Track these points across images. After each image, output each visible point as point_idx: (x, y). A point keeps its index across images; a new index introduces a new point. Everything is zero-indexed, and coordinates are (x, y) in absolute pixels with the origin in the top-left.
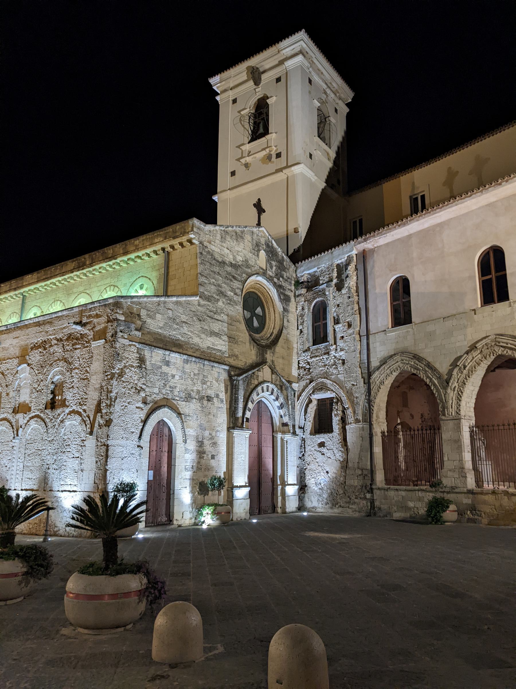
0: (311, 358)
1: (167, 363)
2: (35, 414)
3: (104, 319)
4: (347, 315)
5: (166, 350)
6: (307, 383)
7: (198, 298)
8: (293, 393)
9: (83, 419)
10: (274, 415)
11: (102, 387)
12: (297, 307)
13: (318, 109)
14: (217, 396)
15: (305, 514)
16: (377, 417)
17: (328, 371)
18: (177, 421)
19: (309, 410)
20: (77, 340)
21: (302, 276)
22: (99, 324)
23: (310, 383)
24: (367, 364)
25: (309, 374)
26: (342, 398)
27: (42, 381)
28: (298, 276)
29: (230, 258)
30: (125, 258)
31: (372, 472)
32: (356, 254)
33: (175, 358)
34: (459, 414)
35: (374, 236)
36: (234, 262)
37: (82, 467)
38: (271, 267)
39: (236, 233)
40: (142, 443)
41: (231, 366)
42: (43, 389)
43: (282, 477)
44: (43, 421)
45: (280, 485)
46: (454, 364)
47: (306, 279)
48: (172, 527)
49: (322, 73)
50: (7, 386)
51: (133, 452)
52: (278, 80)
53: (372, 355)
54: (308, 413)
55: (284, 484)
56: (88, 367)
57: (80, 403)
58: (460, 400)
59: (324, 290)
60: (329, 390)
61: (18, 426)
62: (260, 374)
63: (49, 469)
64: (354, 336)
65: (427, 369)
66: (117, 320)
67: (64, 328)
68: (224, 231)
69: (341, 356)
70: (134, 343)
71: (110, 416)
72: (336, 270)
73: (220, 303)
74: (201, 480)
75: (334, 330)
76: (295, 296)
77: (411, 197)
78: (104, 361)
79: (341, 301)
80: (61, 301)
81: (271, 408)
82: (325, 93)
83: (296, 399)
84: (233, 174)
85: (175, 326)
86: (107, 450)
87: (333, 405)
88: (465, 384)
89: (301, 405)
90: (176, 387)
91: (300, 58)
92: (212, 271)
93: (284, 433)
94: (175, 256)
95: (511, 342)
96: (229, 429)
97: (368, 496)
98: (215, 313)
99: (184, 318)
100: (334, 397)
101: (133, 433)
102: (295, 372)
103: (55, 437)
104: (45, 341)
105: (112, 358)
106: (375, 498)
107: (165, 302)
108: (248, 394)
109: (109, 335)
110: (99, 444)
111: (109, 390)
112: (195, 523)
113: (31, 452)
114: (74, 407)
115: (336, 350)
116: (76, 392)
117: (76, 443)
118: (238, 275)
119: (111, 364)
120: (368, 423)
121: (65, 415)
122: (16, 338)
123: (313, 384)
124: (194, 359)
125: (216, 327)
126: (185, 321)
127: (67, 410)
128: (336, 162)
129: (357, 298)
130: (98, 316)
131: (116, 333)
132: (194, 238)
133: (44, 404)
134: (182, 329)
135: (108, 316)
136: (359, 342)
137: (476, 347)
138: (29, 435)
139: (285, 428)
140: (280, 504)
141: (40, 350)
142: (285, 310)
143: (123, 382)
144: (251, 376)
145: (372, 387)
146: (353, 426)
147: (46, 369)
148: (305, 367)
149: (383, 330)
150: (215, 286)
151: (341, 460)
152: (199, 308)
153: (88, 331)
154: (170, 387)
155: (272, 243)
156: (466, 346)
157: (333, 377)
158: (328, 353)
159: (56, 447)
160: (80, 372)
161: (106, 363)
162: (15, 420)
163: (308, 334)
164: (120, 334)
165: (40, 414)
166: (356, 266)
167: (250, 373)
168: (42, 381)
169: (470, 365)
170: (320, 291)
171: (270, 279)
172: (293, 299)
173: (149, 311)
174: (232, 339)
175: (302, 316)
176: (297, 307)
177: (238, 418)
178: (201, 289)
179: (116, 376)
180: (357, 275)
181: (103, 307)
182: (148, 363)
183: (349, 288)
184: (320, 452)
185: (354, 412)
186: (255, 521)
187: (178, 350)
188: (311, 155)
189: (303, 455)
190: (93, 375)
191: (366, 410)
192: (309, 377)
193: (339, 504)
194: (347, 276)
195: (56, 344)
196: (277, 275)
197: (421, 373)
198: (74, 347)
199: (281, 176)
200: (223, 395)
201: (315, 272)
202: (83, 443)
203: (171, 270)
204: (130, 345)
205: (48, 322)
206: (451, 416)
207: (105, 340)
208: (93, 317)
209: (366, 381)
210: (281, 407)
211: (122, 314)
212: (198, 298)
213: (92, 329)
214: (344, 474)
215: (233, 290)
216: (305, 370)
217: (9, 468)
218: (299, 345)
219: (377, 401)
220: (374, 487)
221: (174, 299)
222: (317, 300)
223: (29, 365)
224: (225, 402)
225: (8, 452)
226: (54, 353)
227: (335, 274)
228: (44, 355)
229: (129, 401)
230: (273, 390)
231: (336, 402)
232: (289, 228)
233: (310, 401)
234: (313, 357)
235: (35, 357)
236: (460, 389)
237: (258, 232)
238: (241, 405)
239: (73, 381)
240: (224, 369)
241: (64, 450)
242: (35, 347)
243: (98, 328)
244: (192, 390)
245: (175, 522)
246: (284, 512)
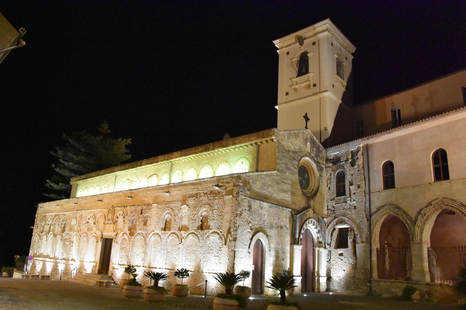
0: (335, 204)
1: (262, 208)
2: (192, 232)
3: (232, 184)
4: (358, 180)
5: (261, 201)
6: (332, 218)
7: (276, 172)
8: (325, 224)
9: (220, 236)
10: (314, 236)
11: (231, 220)
12: (327, 174)
13: (336, 59)
14: (285, 226)
15: (331, 293)
16: (375, 240)
17: (345, 212)
18: (266, 239)
19: (334, 234)
20: (216, 194)
21: (330, 156)
22: (228, 187)
23: (334, 219)
24: (369, 209)
26: (354, 228)
27: (195, 214)
28: (328, 155)
29: (292, 148)
30: (234, 147)
31: (371, 271)
32: (363, 146)
33: (265, 205)
34: (422, 241)
35: (373, 137)
36: (294, 150)
37: (220, 261)
38: (313, 152)
39: (295, 133)
40: (250, 251)
41: (292, 209)
42: (196, 219)
43: (318, 272)
44: (197, 235)
45: (317, 276)
46: (419, 213)
47: (332, 158)
48: (264, 295)
49: (338, 39)
50: (174, 216)
51: (246, 255)
52: (314, 43)
53: (372, 205)
54: (333, 236)
55: (319, 276)
56: (223, 209)
58: (422, 233)
59: (343, 165)
60: (346, 224)
62: (308, 213)
63: (200, 261)
64: (361, 193)
65: (404, 215)
66: (239, 185)
67: (208, 187)
68: (289, 133)
69: (353, 204)
70: (247, 198)
72: (350, 154)
73: (287, 174)
74: (277, 272)
75: (350, 189)
76: (326, 167)
77: (392, 111)
78: (232, 207)
79: (354, 172)
80: (194, 168)
81: (312, 233)
82: (340, 49)
83: (326, 228)
84: (287, 94)
85: (266, 188)
86: (235, 254)
87: (348, 232)
88: (425, 224)
89: (329, 231)
90: (265, 221)
91: (326, 33)
92: (283, 156)
93: (319, 247)
94: (262, 147)
95: (451, 202)
96: (291, 244)
97: (368, 284)
98: (285, 180)
99: (270, 183)
100: (349, 228)
101: (246, 245)
102: (325, 212)
103: (204, 244)
104: (197, 194)
105: (237, 205)
106: (372, 286)
107: (261, 175)
108: (301, 225)
109: (234, 194)
110: (230, 250)
111: (236, 222)
112: (274, 294)
114: (215, 230)
115: (351, 200)
116: (216, 222)
117: (216, 249)
118: (296, 157)
119: (236, 208)
120: (369, 244)
122: (180, 190)
123: (336, 220)
124: (274, 206)
125: (285, 187)
126: (270, 184)
127: (211, 231)
128: (347, 88)
129: (363, 171)
130: (228, 183)
131: (239, 192)
132: (275, 139)
134: (268, 189)
135: (234, 183)
136: (365, 197)
137: (431, 204)
138: (188, 242)
139: (320, 244)
140: (316, 287)
142: (321, 176)
143: (242, 218)
144: (303, 215)
145: (371, 223)
146: (360, 245)
147: (198, 209)
148: (331, 209)
149: (378, 191)
150: (285, 164)
151: (353, 264)
152: (277, 177)
153: (222, 190)
154: (263, 221)
155: (313, 137)
156: (425, 203)
157: (349, 216)
158: (346, 202)
161: (233, 208)
162: (180, 234)
163: (333, 190)
164: (240, 193)
165: (194, 232)
166: (362, 153)
167: (303, 213)
168: (195, 214)
169: (428, 213)
170: (341, 165)
171: (312, 158)
172: (324, 169)
173: (254, 180)
174: (293, 193)
175: (330, 179)
176: (327, 174)
177: (296, 238)
178: (278, 167)
179: (239, 215)
180: (363, 158)
181: (231, 178)
182: (253, 208)
183: (359, 165)
184: (340, 259)
185: (361, 237)
186: (305, 295)
187: (266, 201)
188: (333, 86)
189: (330, 260)
190: (225, 214)
191: (368, 236)
192: (334, 215)
193: (351, 289)
194: (357, 159)
195: (203, 196)
196: (316, 156)
197: (400, 216)
198: (214, 198)
199: (316, 97)
200: (288, 226)
201: (338, 154)
203: (260, 155)
204: (245, 199)
205: (199, 184)
206: (417, 242)
207: (233, 196)
208: (225, 183)
209: (369, 219)
210: (318, 232)
211: (242, 182)
212: (276, 172)
213: (225, 189)
214: (354, 272)
215: (293, 166)
216: (331, 211)
217: (177, 259)
218: (328, 196)
219: (375, 231)
220: (372, 279)
221: (265, 173)
222: (339, 170)
223: (187, 205)
224: (289, 230)
225: (176, 250)
226: (202, 200)
227: (350, 157)
228: (196, 201)
229: (244, 228)
230: (314, 222)
231: (350, 231)
232: (322, 127)
233: (334, 229)
234: (337, 204)
235: (191, 201)
236: (422, 227)
237: (306, 132)
238: (298, 231)
239: (214, 216)
240: (289, 211)
241: (209, 252)
242: (191, 196)
243: (228, 189)
244: (273, 223)
245: (265, 293)
246: (319, 291)
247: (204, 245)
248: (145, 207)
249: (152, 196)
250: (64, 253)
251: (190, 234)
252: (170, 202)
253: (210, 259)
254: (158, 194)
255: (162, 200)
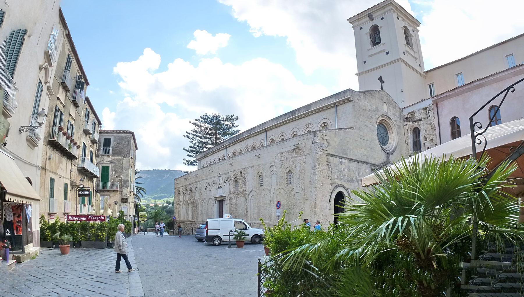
36: (371, 109)
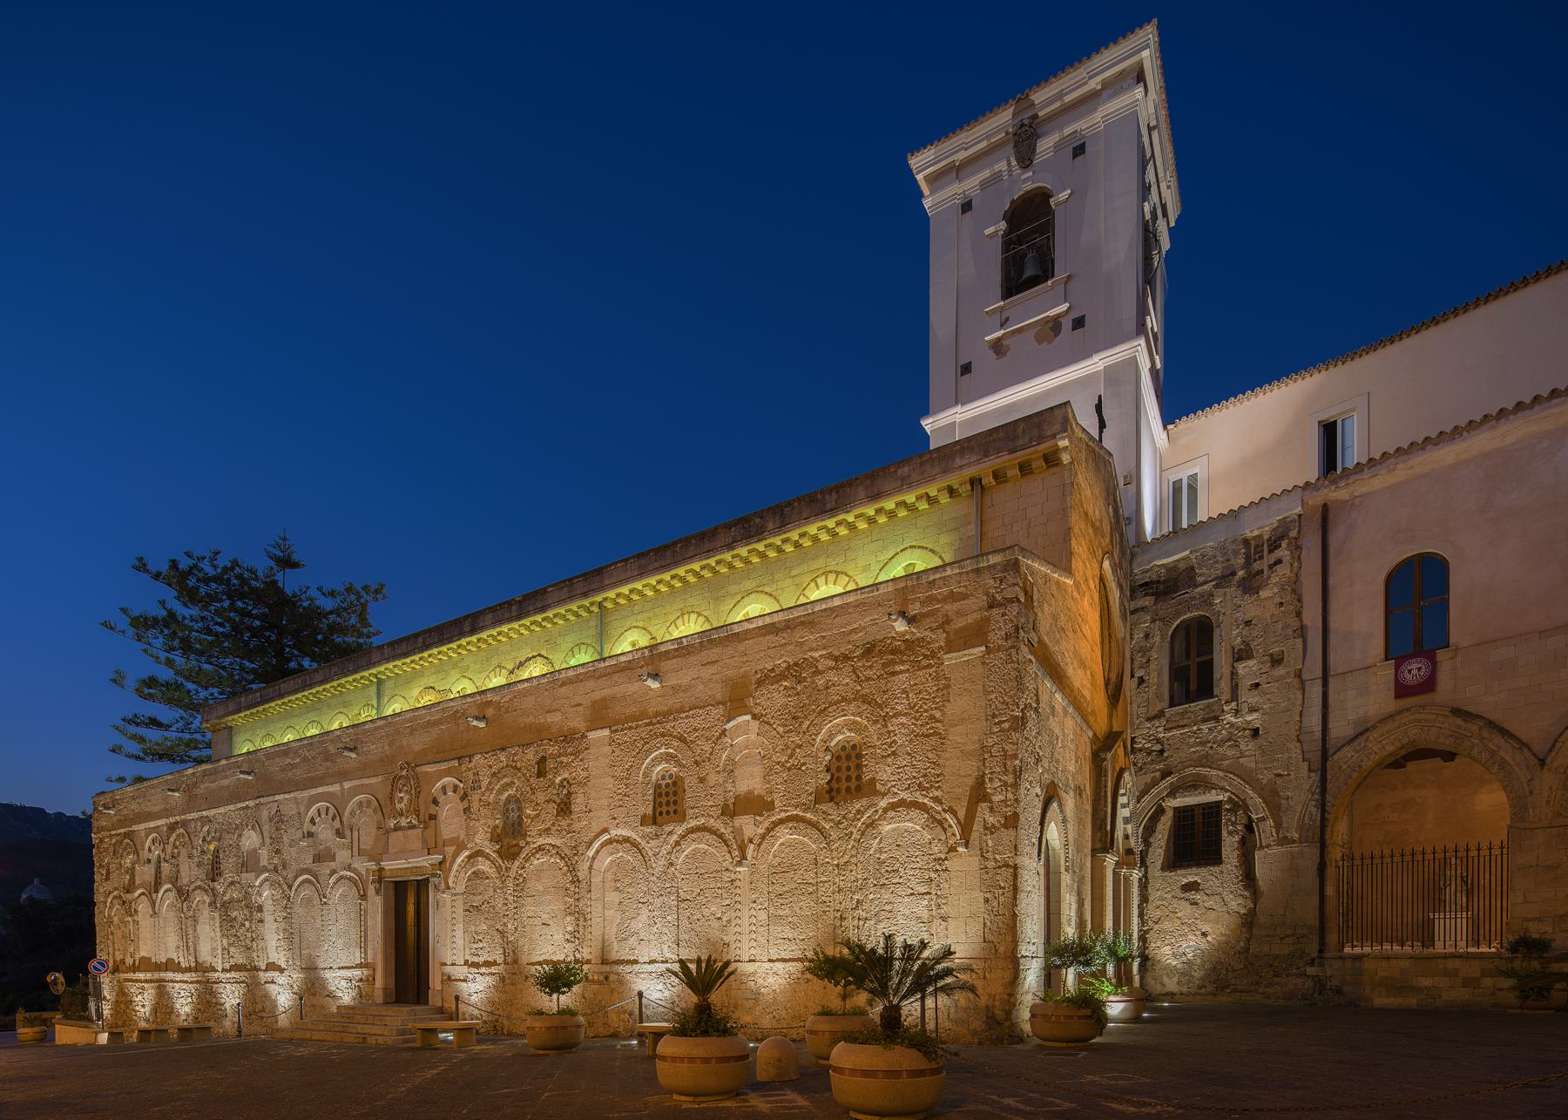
2: (788, 814)
9: (932, 817)
25: (1160, 762)
27: (800, 747)
42: (804, 764)
44: (814, 825)
50: (696, 763)
57: (920, 785)
61: (743, 841)
63: (842, 918)
71: (1015, 808)
86: (1015, 877)
113: (784, 889)
121: (877, 811)
127: (883, 804)
133: (811, 794)
141: (786, 683)
147: (808, 723)
159: (859, 876)
160: (913, 721)
165: (801, 814)
168: (800, 747)
190: (952, 726)
202: (940, 864)
216: (1149, 754)
223: (755, 717)
228: (798, 694)
235: (774, 699)
241: (883, 881)
247: (854, 860)
248: (552, 750)
249: (580, 705)
250: (232, 949)
251: (781, 822)
252: (665, 715)
253: (888, 907)
254: (607, 692)
255: (632, 710)
